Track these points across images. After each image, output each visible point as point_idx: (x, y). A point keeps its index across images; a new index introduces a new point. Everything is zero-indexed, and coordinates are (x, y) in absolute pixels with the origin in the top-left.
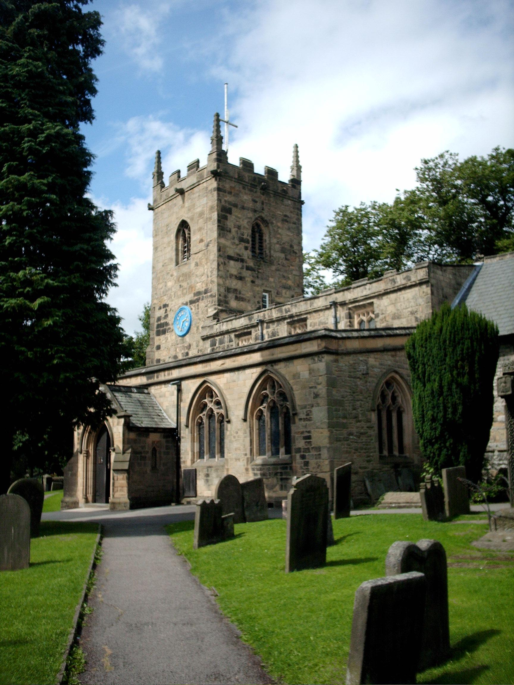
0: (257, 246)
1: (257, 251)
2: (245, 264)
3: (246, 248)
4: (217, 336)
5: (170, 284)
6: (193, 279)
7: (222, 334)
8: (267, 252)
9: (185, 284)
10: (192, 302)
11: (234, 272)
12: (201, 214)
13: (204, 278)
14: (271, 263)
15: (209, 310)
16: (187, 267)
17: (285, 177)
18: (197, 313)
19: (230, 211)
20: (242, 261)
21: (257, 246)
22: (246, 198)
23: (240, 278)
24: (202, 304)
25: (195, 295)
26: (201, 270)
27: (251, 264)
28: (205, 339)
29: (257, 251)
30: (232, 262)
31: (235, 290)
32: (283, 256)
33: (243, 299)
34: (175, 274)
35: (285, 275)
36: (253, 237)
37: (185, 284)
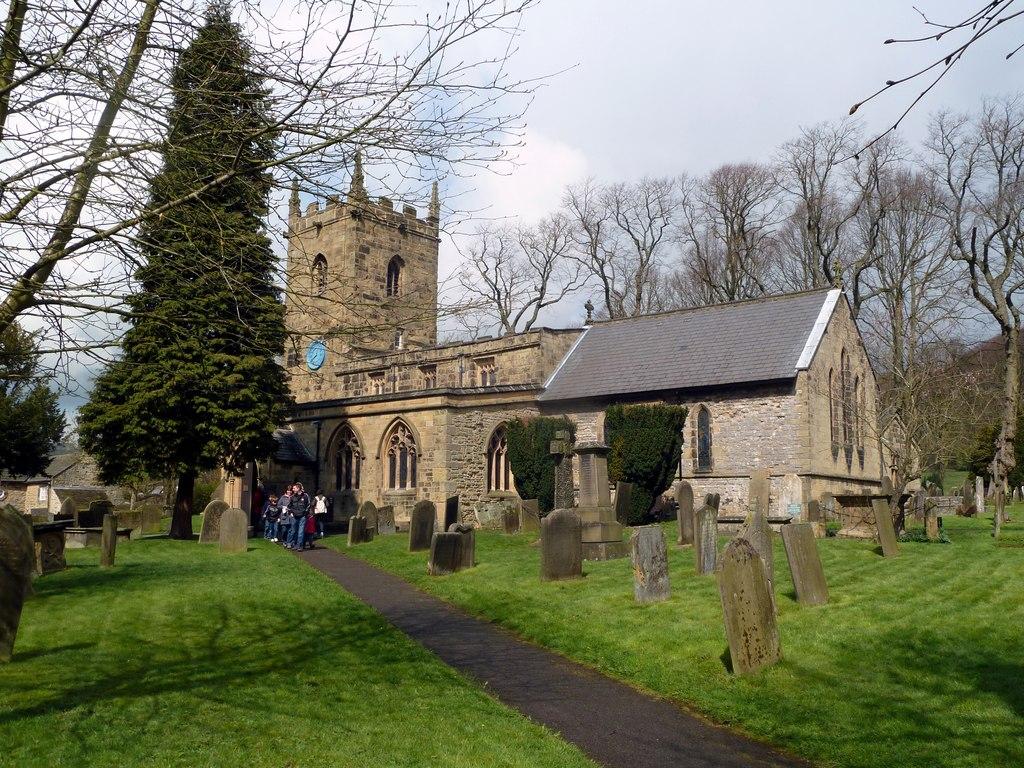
7: (356, 372)
12: (339, 251)
17: (422, 214)
19: (367, 251)
20: (378, 299)
22: (384, 236)
36: (389, 276)
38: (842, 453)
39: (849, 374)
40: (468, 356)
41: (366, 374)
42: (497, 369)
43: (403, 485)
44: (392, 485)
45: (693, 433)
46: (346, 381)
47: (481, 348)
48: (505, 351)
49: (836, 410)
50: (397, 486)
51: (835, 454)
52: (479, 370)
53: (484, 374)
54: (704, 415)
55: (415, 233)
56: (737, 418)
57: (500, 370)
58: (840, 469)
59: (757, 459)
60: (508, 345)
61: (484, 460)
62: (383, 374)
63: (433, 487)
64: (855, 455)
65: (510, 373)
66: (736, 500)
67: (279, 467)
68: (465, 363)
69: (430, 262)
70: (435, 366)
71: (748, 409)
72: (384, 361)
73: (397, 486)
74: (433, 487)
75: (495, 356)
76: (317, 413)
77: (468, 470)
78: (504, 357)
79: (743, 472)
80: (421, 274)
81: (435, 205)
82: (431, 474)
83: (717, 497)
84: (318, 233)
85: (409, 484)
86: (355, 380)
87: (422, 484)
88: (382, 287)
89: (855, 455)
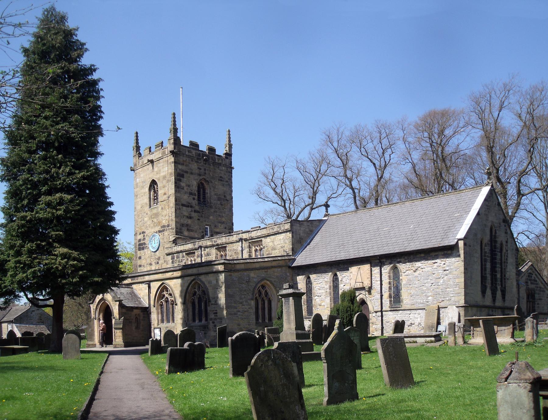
0: (202, 197)
1: (202, 200)
2: (193, 209)
3: (194, 199)
4: (175, 253)
5: (146, 219)
6: (160, 218)
7: (178, 252)
8: (209, 200)
9: (155, 220)
10: (160, 232)
11: (186, 214)
13: (167, 218)
14: (211, 207)
15: (171, 237)
16: (156, 209)
17: (221, 151)
18: (163, 239)
20: (191, 207)
21: (202, 197)
22: (194, 166)
23: (190, 218)
24: (166, 233)
25: (162, 227)
26: (165, 213)
27: (197, 208)
28: (168, 254)
29: (202, 200)
30: (184, 208)
31: (187, 225)
32: (219, 202)
33: (192, 231)
34: (149, 213)
35: (220, 214)
36: (199, 191)
37: (155, 220)
38: (489, 292)
39: (496, 242)
40: (246, 240)
41: (184, 254)
42: (264, 247)
43: (200, 320)
44: (194, 320)
45: (390, 283)
46: (173, 258)
47: (254, 234)
48: (269, 235)
49: (485, 265)
50: (197, 321)
51: (484, 292)
52: (253, 249)
53: (256, 250)
54: (396, 272)
55: (214, 163)
56: (418, 272)
57: (266, 248)
58: (488, 301)
59: (430, 298)
60: (271, 231)
61: (253, 303)
62: (194, 253)
63: (218, 320)
64: (499, 294)
65: (272, 250)
66: (417, 324)
67: (124, 310)
68: (245, 244)
69: (227, 182)
70: (226, 247)
71: (424, 266)
72: (194, 245)
73: (197, 321)
74: (218, 320)
75: (263, 239)
76: (147, 278)
77: (241, 310)
78: (268, 239)
79: (421, 306)
80: (220, 189)
81: (230, 146)
82: (216, 313)
83: (403, 323)
84: (153, 166)
85: (204, 319)
86: (178, 257)
87: (211, 319)
88: (194, 199)
89: (499, 294)
